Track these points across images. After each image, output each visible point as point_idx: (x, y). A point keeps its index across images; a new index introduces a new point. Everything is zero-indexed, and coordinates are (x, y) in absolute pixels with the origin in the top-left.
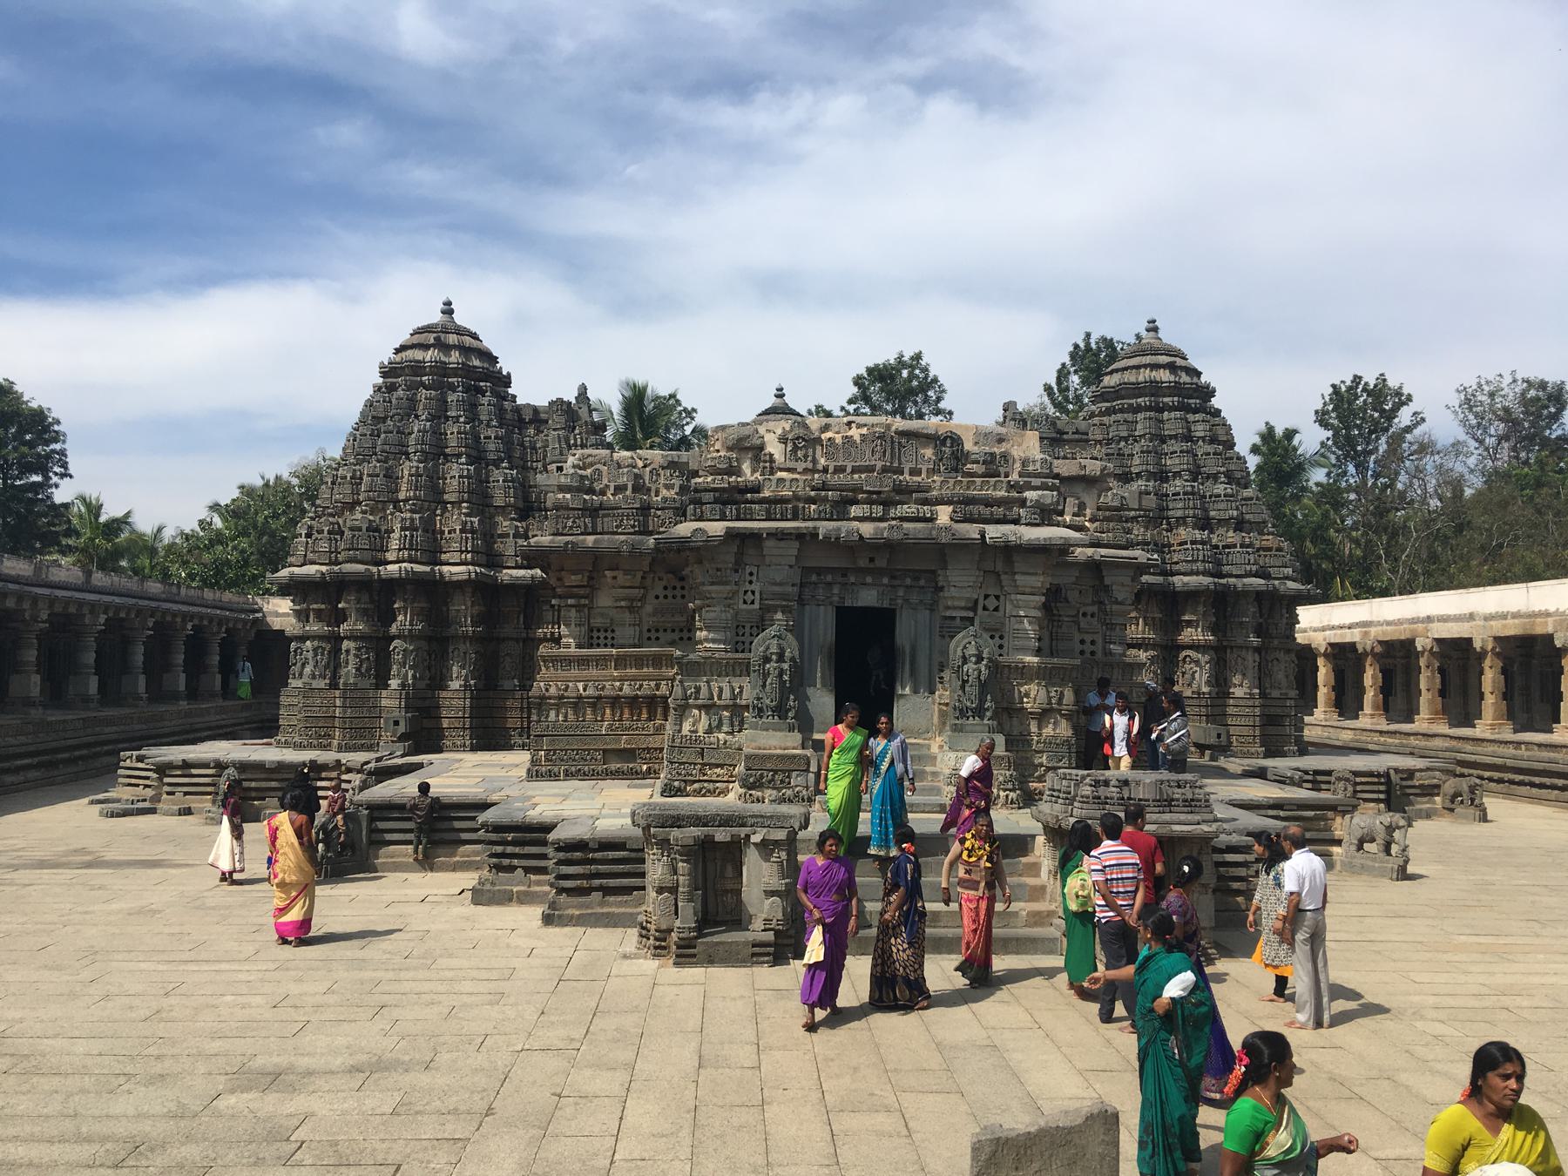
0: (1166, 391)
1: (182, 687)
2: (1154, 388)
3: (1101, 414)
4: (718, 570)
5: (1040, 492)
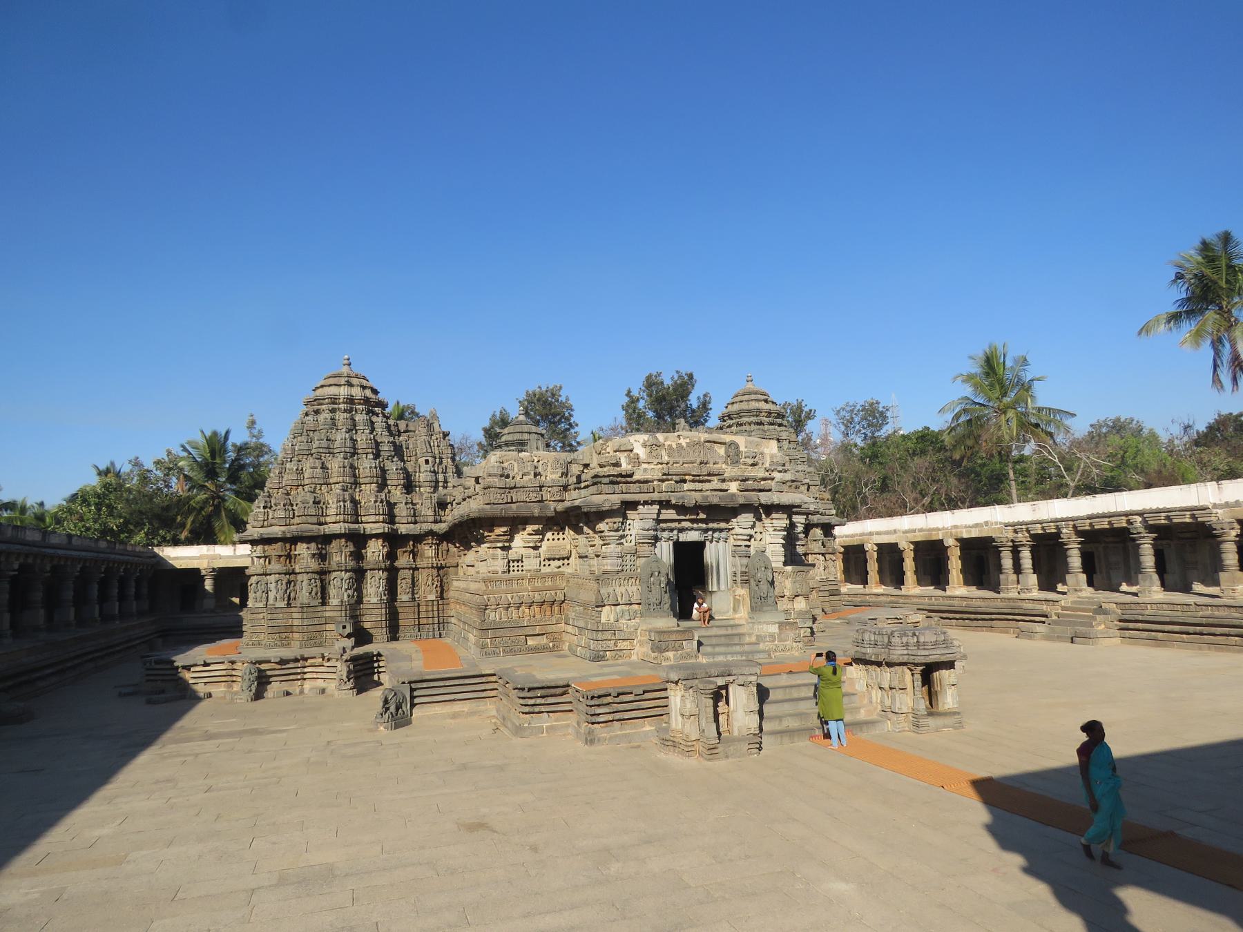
0: (763, 413)
1: (117, 612)
2: (759, 411)
3: (730, 426)
4: (615, 523)
5: (782, 474)
